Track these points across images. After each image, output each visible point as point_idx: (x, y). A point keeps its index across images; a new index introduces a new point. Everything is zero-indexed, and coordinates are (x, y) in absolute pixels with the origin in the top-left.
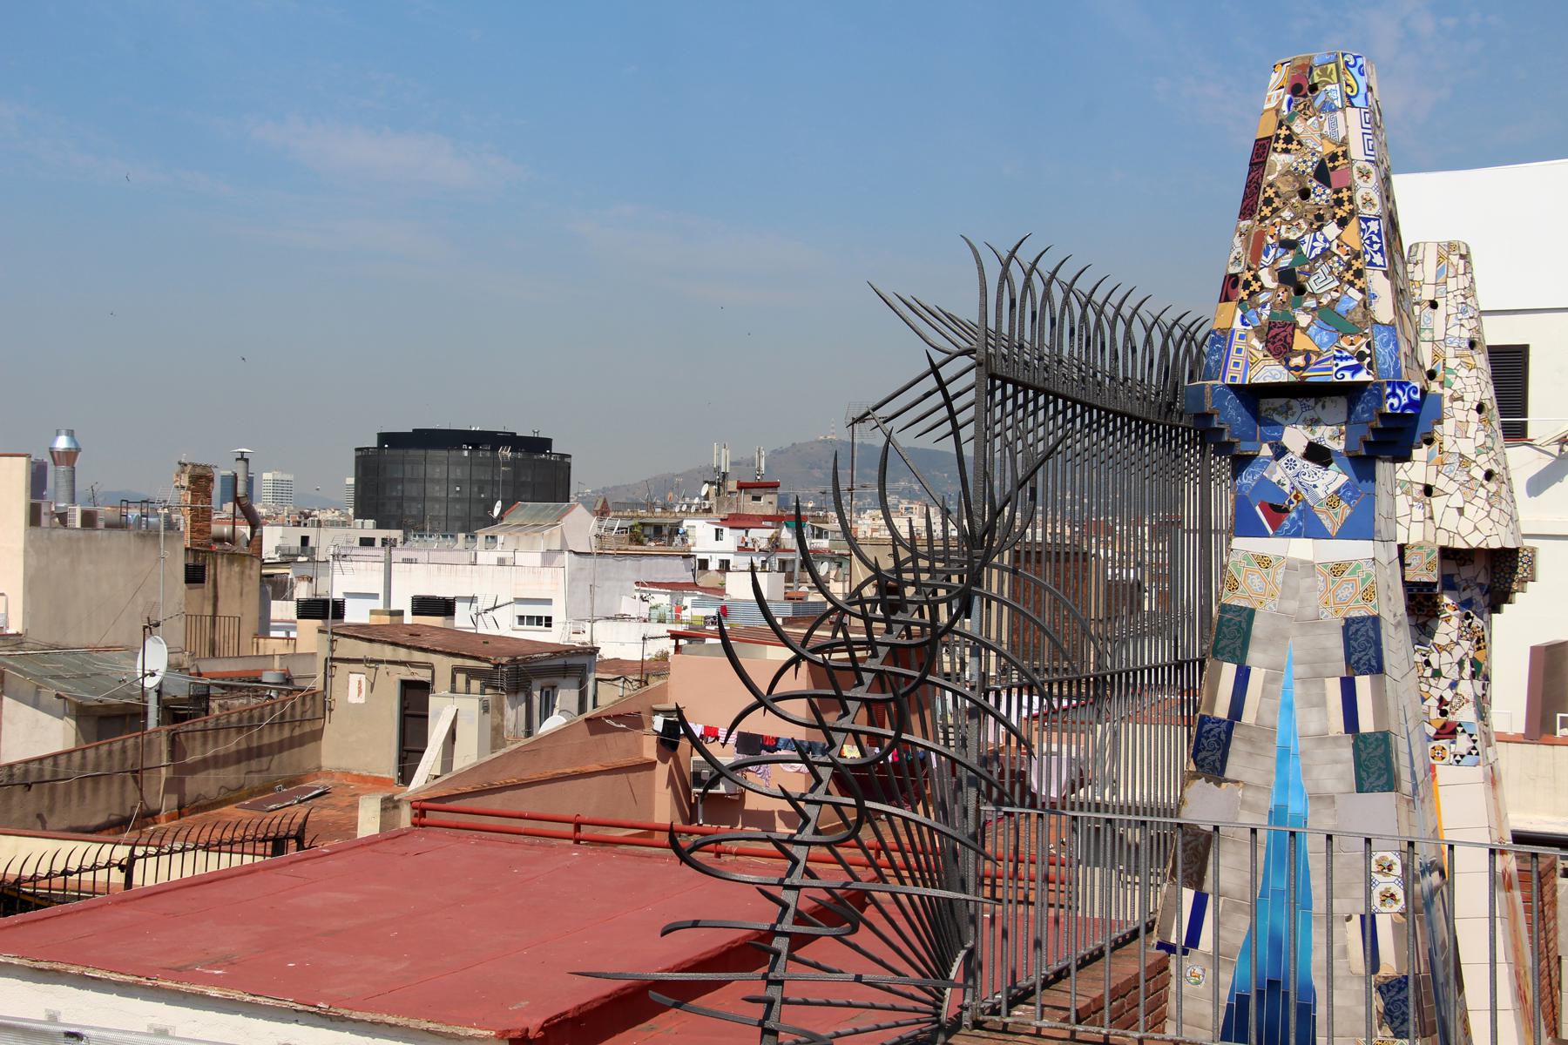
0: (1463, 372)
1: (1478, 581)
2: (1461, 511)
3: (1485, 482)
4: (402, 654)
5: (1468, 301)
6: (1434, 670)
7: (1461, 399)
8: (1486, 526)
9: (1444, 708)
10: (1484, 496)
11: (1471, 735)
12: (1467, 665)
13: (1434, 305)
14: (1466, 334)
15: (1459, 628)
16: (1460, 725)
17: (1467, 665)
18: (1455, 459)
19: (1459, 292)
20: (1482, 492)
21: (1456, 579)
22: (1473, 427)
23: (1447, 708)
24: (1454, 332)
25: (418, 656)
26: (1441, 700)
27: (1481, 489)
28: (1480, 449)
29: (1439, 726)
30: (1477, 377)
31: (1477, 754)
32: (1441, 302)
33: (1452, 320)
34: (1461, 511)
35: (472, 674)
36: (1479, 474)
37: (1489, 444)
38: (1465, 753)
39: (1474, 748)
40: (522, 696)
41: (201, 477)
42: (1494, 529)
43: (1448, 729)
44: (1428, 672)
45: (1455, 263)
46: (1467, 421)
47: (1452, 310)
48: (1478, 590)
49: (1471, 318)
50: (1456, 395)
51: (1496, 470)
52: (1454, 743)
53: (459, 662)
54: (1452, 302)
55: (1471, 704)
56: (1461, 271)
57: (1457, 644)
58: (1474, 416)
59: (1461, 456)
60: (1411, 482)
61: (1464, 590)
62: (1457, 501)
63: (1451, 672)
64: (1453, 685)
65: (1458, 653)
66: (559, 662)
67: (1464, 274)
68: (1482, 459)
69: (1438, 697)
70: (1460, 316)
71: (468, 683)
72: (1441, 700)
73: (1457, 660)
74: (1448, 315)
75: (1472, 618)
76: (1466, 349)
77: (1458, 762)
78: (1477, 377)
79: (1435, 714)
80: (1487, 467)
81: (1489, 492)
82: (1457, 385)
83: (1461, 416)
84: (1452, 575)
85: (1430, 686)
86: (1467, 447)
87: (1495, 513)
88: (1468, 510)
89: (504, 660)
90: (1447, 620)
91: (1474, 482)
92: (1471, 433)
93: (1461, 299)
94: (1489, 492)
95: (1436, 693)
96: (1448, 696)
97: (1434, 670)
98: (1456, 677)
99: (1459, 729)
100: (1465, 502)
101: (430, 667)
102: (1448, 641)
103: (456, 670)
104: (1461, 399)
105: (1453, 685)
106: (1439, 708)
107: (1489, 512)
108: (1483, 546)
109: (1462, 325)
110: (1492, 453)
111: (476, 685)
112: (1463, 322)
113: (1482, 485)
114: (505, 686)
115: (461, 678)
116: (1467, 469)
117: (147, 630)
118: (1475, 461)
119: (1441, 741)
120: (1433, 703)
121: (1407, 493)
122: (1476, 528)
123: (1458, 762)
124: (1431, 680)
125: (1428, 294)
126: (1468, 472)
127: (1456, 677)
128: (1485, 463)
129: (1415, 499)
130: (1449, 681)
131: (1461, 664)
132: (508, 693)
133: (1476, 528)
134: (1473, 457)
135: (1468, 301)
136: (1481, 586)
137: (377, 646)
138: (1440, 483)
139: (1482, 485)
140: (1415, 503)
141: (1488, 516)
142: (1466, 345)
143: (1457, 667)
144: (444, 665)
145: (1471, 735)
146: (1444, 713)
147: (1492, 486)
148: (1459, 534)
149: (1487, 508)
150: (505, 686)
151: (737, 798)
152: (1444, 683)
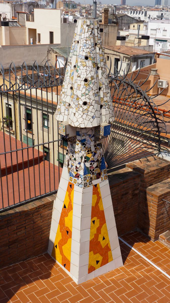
0: (81, 68)
1: (88, 133)
2: (75, 114)
3: (82, 106)
4: (115, 53)
5: (87, 42)
6: (74, 158)
7: (80, 77)
8: (80, 120)
9: (77, 169)
10: (82, 110)
11: (82, 179)
12: (83, 158)
13: (78, 42)
14: (84, 54)
15: (81, 147)
16: (80, 175)
17: (83, 158)
18: (75, 97)
19: (84, 39)
20: (81, 109)
21: (80, 133)
22: (82, 87)
23: (78, 169)
24: (81, 53)
25: (118, 54)
26: (76, 167)
27: (81, 108)
28: (83, 94)
29: (76, 174)
30: (86, 70)
31: (82, 185)
32: (80, 41)
33: (81, 49)
34: (75, 114)
35: (126, 58)
36: (81, 103)
37: (87, 92)
38: (80, 184)
39: (79, 184)
40: (136, 63)
41: (106, 10)
42: (83, 122)
43: (77, 175)
44: (73, 159)
45: (85, 28)
46: (81, 85)
47: (82, 45)
48: (88, 136)
49: (87, 48)
50: (79, 76)
51: (88, 101)
52: (78, 180)
53: (124, 55)
54: (82, 42)
55: (83, 170)
56: (86, 31)
57: (80, 152)
58: (83, 83)
59: (77, 96)
60: (66, 102)
61: (83, 136)
62: (74, 111)
63: (79, 160)
64: (80, 163)
65: (81, 154)
66: (146, 55)
67: (87, 32)
68: (84, 97)
69: (75, 166)
70: (83, 47)
71: (126, 60)
72: (76, 167)
73: (80, 156)
74: (80, 47)
75: (86, 145)
76: (84, 59)
77: (78, 185)
78: (86, 70)
79: (75, 170)
80: (85, 100)
81: (83, 109)
82: (79, 72)
83: (79, 83)
84: (79, 132)
85: (74, 162)
86: (79, 93)
87: (84, 116)
88: (77, 114)
89: (132, 56)
90: (78, 144)
91: (79, 105)
92: (81, 89)
93: (85, 41)
94: (83, 109)
95: (75, 165)
96: (78, 166)
97: (74, 158)
98: (80, 161)
99: (80, 176)
100: (76, 111)
101: (120, 56)
102: (78, 151)
103: (124, 57)
104: (80, 77)
105: (80, 163)
106: (76, 169)
107: (82, 116)
108: (79, 126)
109: (84, 51)
110: (88, 96)
111: (127, 60)
112: (84, 50)
113: (81, 107)
114: (132, 61)
115: (125, 58)
116: (78, 101)
117: (48, 52)
118: (81, 98)
119: (76, 178)
120: (74, 167)
121: (64, 105)
122: (77, 121)
123: (78, 185)
124: (74, 161)
125: (77, 38)
126: (78, 102)
127: (80, 161)
128: (84, 99)
129: (66, 108)
130: (78, 162)
131: (82, 158)
132: (133, 62)
133: (77, 121)
134: (80, 97)
135: (87, 42)
136: (89, 135)
137: (111, 51)
138: (72, 104)
139: (81, 107)
140: (66, 109)
141: (82, 117)
142: (84, 58)
143: (80, 158)
144: (122, 55)
145: (82, 179)
146: (77, 171)
147: (85, 107)
148: (73, 122)
149: (82, 114)
150: (132, 61)
151: (167, 89)
152: (77, 162)
